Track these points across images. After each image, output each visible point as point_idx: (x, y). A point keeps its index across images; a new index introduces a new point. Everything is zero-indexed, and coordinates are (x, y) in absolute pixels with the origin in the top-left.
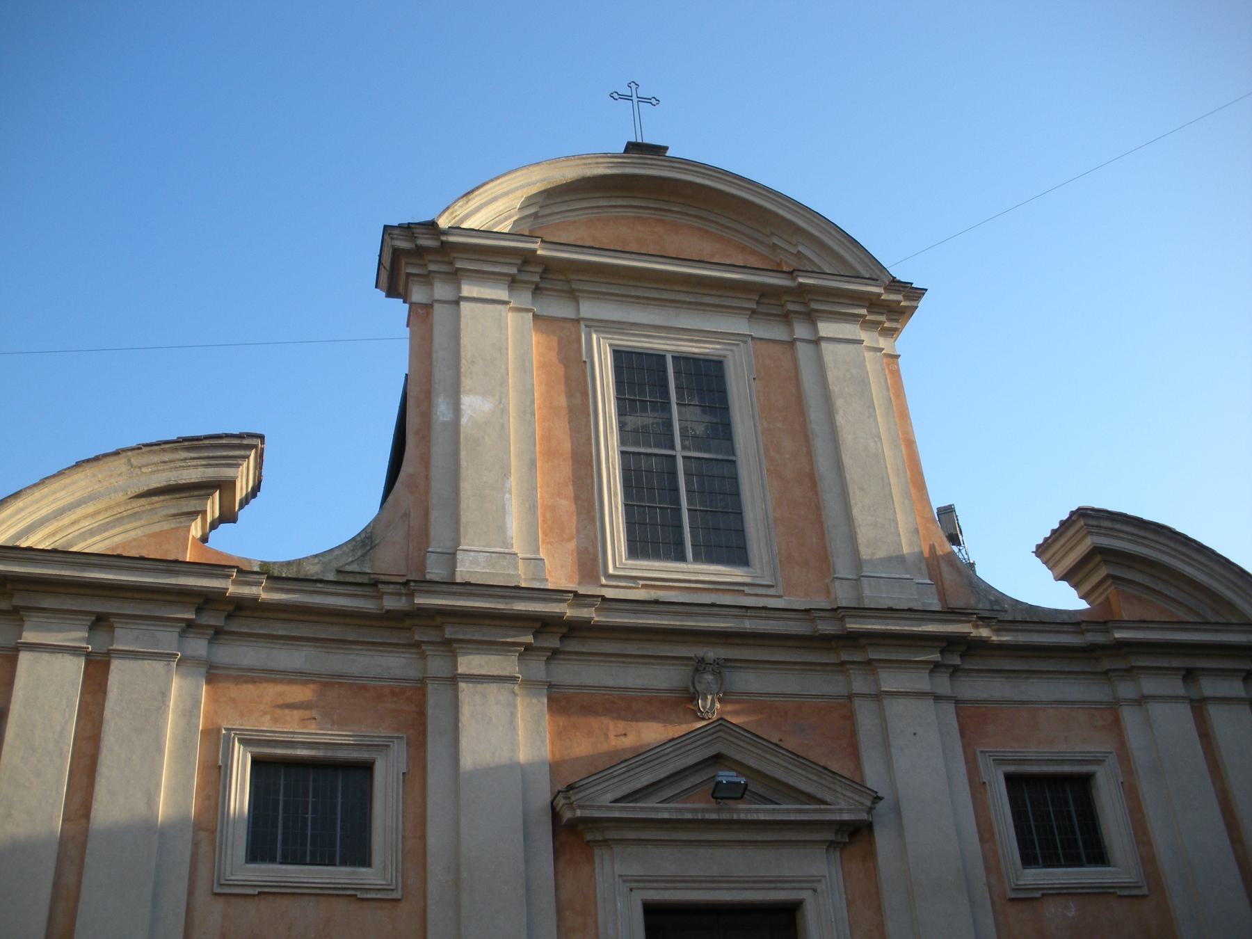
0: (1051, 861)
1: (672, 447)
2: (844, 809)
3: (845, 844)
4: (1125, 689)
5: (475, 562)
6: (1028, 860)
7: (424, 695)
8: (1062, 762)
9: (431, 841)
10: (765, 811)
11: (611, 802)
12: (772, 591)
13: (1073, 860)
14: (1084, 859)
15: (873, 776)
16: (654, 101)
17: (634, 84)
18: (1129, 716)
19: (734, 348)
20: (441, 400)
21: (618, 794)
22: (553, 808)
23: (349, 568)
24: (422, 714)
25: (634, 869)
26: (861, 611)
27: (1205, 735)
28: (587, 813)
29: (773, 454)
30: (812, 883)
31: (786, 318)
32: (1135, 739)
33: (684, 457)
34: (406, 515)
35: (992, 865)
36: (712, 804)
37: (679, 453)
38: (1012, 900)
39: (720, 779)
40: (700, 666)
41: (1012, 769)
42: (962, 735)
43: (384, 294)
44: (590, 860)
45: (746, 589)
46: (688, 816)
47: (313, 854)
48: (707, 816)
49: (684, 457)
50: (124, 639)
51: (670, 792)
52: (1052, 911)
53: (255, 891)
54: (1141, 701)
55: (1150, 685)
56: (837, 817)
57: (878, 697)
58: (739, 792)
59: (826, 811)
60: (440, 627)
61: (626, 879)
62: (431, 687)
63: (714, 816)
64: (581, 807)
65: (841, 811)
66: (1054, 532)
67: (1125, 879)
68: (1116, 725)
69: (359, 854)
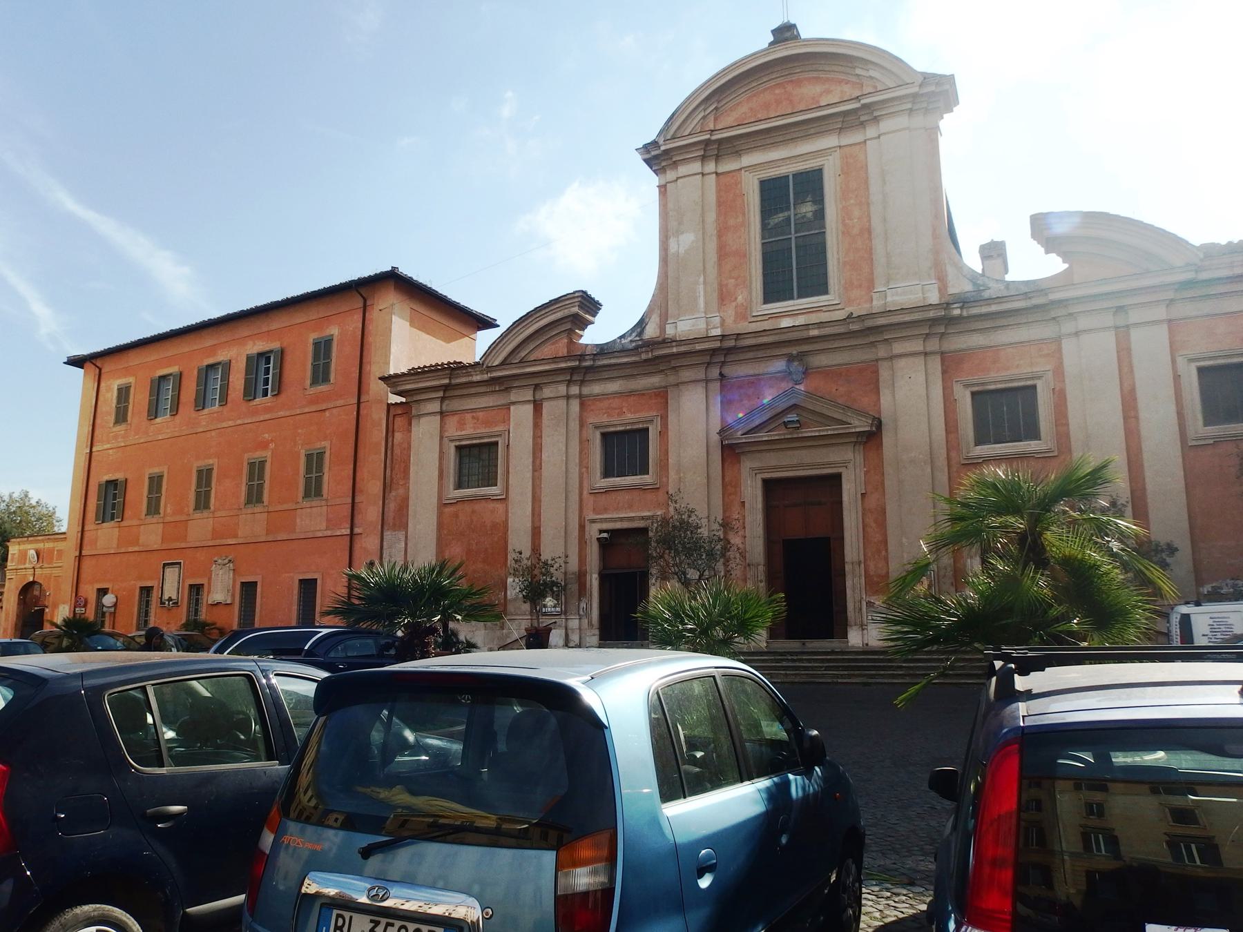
1: (791, 234)
3: (866, 442)
8: (1012, 381)
12: (839, 307)
19: (828, 158)
21: (745, 431)
25: (757, 464)
28: (730, 442)
30: (845, 464)
31: (862, 125)
38: (963, 464)
44: (739, 462)
45: (824, 309)
47: (617, 473)
48: (787, 437)
50: (547, 392)
51: (773, 426)
56: (858, 430)
58: (800, 425)
60: (669, 362)
61: (752, 469)
63: (789, 436)
64: (727, 440)
65: (855, 427)
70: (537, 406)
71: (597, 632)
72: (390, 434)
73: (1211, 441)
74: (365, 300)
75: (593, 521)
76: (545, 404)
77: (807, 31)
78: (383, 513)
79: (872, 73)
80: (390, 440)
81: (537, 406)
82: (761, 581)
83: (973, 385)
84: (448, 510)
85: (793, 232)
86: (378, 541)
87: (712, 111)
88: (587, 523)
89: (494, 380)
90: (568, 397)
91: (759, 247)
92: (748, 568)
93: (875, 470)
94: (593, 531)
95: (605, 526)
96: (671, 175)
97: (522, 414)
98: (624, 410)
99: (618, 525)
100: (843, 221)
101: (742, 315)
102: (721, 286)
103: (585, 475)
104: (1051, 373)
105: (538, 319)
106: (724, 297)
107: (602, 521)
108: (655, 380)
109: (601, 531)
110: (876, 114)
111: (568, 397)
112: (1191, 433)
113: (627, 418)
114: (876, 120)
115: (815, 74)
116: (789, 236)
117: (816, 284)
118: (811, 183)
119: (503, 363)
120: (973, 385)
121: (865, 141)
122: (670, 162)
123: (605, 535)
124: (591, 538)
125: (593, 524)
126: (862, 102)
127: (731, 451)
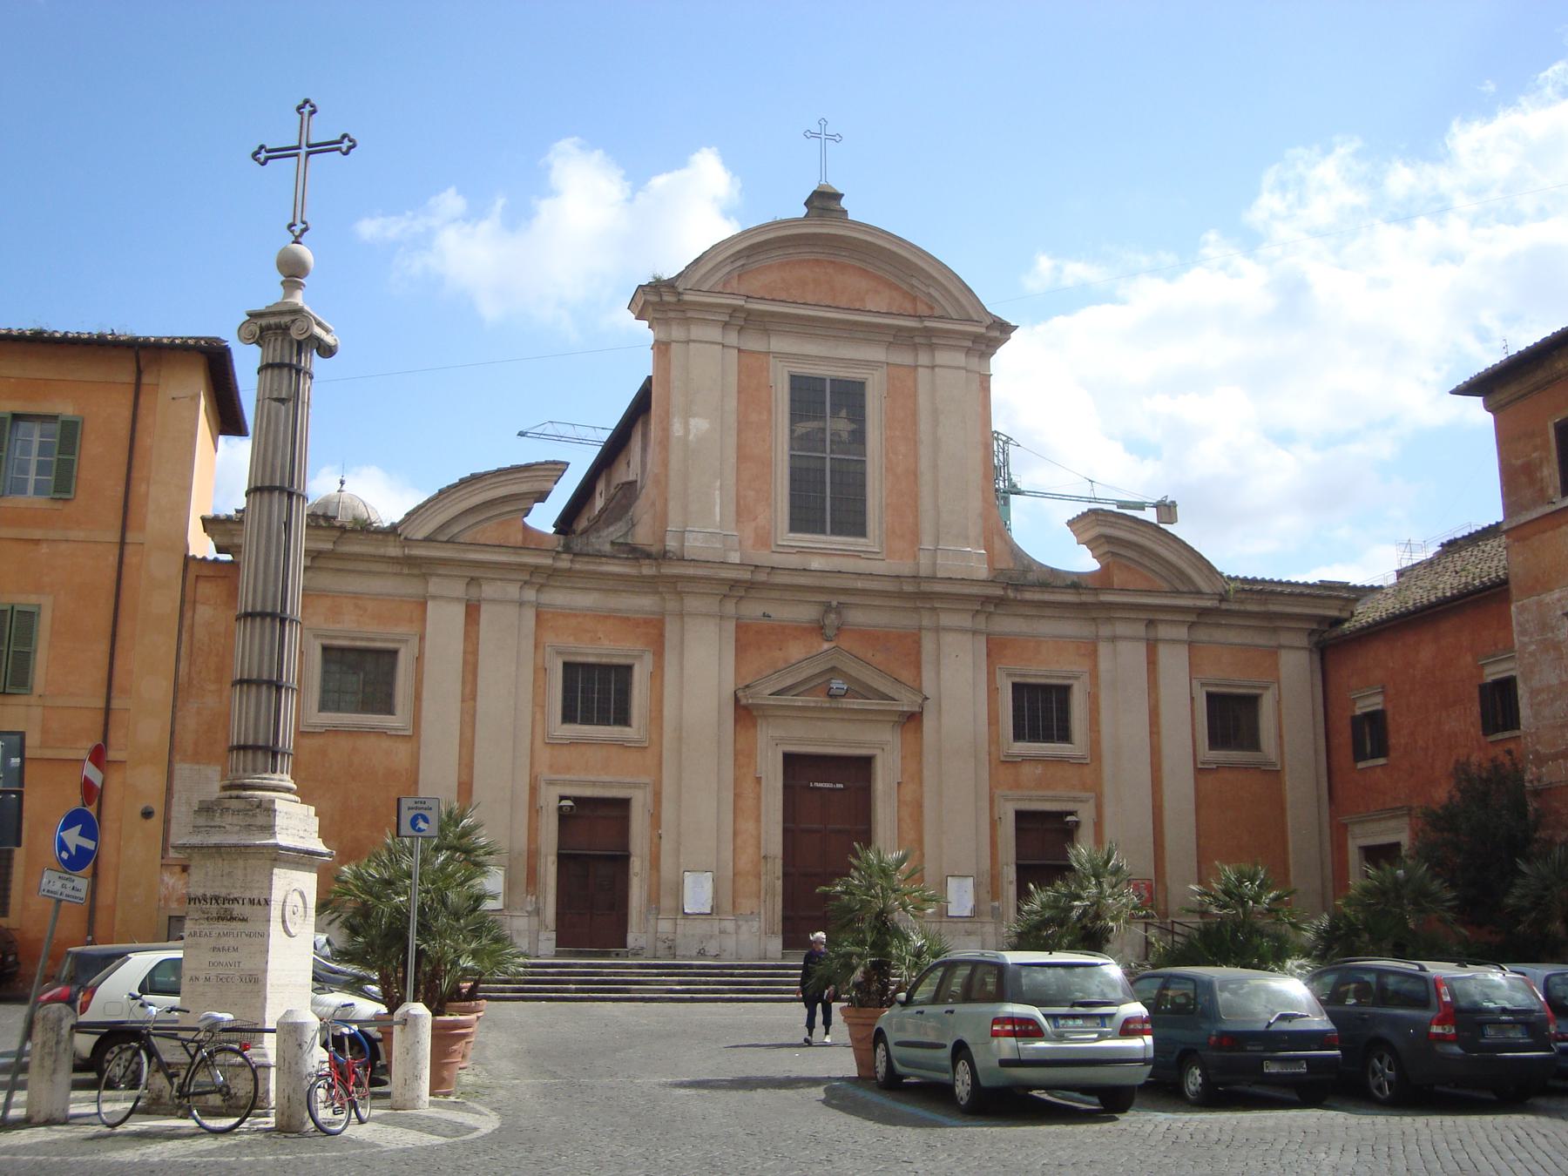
0: (1034, 737)
1: (824, 452)
2: (906, 703)
4: (1105, 630)
5: (695, 539)
6: (1018, 736)
7: (663, 624)
8: (1052, 677)
9: (666, 712)
10: (858, 703)
11: (770, 695)
13: (1048, 738)
14: (1055, 738)
15: (928, 687)
16: (838, 138)
17: (823, 122)
18: (1104, 649)
19: (874, 372)
20: (676, 420)
21: (774, 690)
22: (736, 695)
23: (617, 541)
24: (662, 635)
26: (933, 578)
27: (1152, 662)
28: (755, 701)
29: (891, 455)
31: (915, 347)
32: (1104, 664)
33: (831, 459)
34: (653, 504)
35: (994, 739)
36: (827, 699)
37: (828, 456)
38: (1003, 761)
39: (831, 686)
40: (828, 608)
41: (1017, 680)
42: (988, 655)
43: (634, 316)
44: (755, 725)
45: (862, 555)
46: (812, 705)
49: (831, 459)
50: (488, 590)
52: (1027, 771)
53: (568, 742)
54: (1114, 639)
55: (1121, 629)
56: (900, 709)
57: (938, 630)
59: (893, 705)
62: (668, 619)
64: (751, 697)
66: (1078, 516)
67: (1078, 753)
68: (1093, 655)
69: (623, 718)
70: (473, 612)
71: (553, 935)
72: (187, 606)
73: (1214, 766)
74: (139, 373)
75: (551, 783)
76: (485, 608)
77: (858, 208)
78: (172, 733)
79: (932, 291)
80: (188, 615)
81: (473, 612)
82: (778, 879)
83: (1015, 675)
84: (307, 742)
85: (828, 450)
86: (161, 780)
87: (738, 267)
88: (543, 785)
89: (410, 561)
90: (521, 604)
91: (786, 458)
92: (763, 861)
93: (914, 756)
94: (550, 800)
95: (569, 791)
96: (677, 333)
97: (445, 619)
98: (600, 635)
99: (588, 792)
100: (887, 454)
101: (763, 540)
102: (739, 498)
103: (538, 716)
104: (1087, 674)
105: (492, 486)
106: (742, 512)
107: (565, 783)
108: (644, 603)
109: (562, 798)
110: (934, 340)
111: (521, 604)
112: (1200, 758)
113: (601, 648)
114: (932, 347)
115: (863, 265)
116: (824, 455)
117: (852, 521)
118: (850, 396)
119: (428, 540)
120: (1015, 675)
121: (916, 367)
122: (680, 315)
123: (569, 803)
124: (548, 805)
125: (551, 787)
126: (928, 324)
127: (745, 713)
